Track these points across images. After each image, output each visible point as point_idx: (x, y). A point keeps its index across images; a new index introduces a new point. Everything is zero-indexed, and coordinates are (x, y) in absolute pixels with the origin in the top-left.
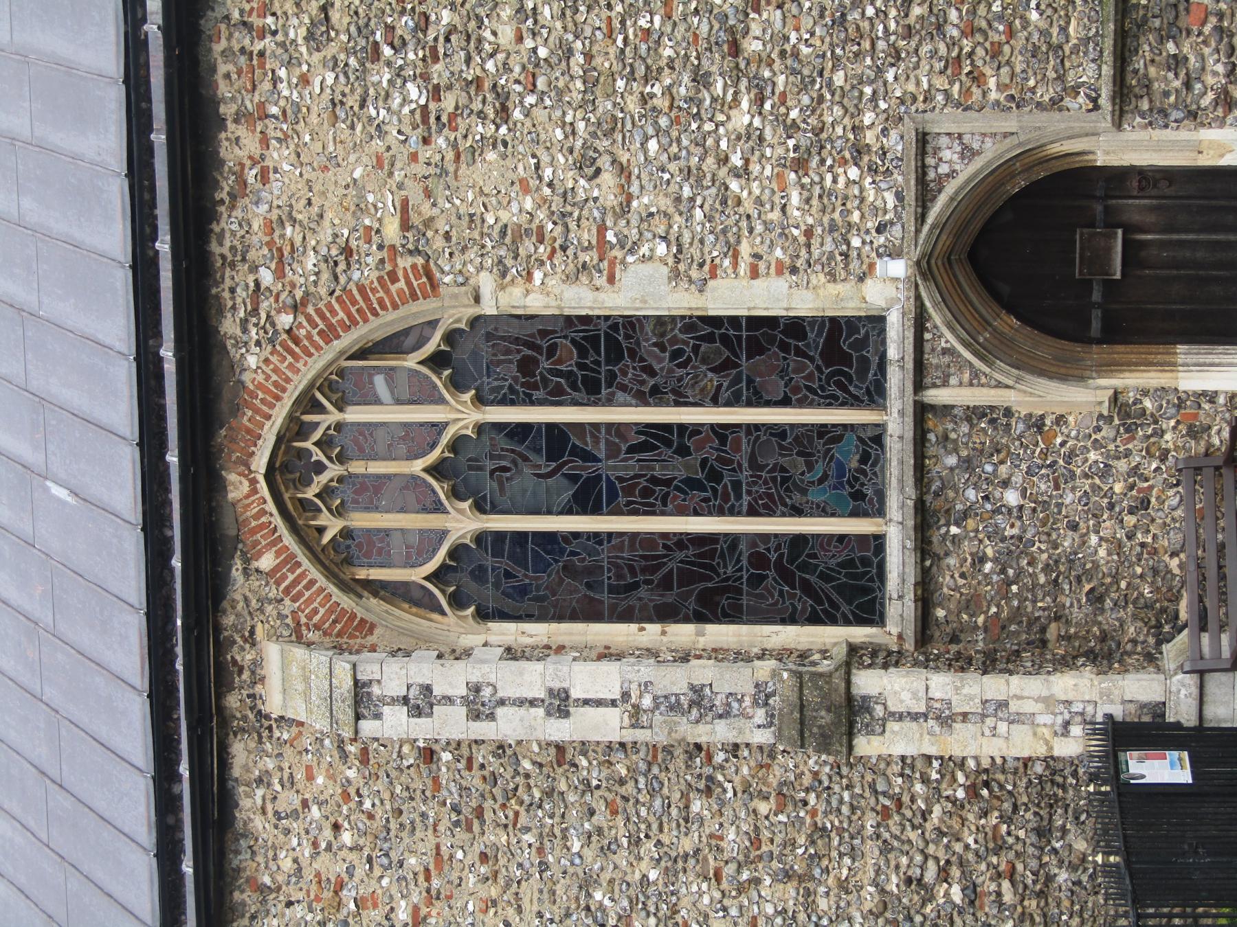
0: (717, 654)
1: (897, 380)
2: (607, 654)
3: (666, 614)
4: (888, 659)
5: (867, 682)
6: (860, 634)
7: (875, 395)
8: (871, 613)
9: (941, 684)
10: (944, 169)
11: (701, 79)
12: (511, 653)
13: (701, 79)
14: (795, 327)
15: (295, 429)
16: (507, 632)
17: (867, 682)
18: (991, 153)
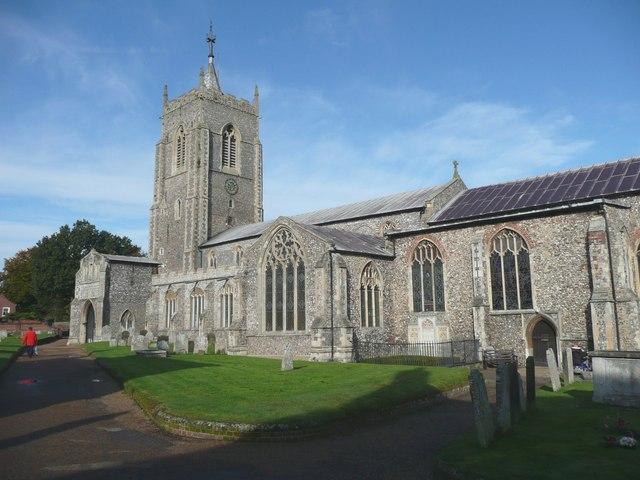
0: (486, 289)
1: (524, 311)
2: (485, 275)
3: (492, 281)
4: (487, 310)
5: (482, 308)
6: (491, 307)
7: (522, 308)
8: (494, 308)
9: (482, 318)
10: (185, 345)
11: (563, 282)
12: (484, 262)
13: (563, 282)
14: (531, 297)
15: (512, 231)
16: (488, 261)
17: (482, 308)
18: (555, 323)
